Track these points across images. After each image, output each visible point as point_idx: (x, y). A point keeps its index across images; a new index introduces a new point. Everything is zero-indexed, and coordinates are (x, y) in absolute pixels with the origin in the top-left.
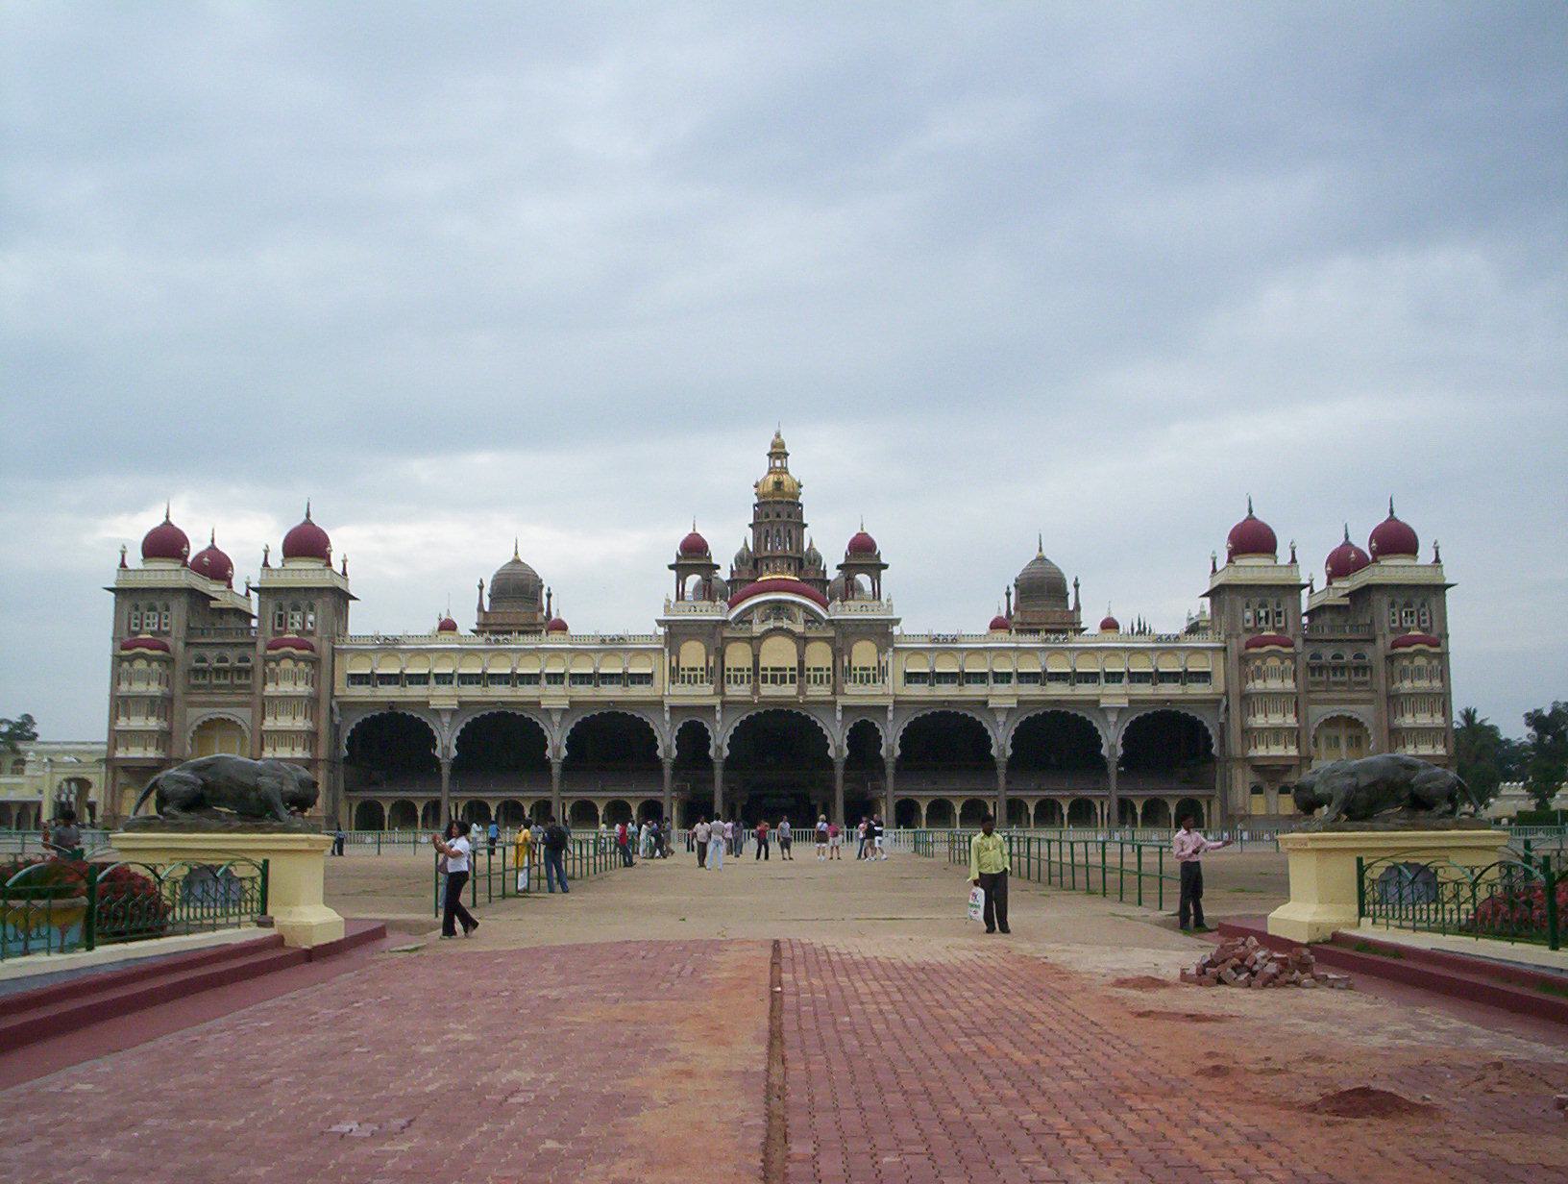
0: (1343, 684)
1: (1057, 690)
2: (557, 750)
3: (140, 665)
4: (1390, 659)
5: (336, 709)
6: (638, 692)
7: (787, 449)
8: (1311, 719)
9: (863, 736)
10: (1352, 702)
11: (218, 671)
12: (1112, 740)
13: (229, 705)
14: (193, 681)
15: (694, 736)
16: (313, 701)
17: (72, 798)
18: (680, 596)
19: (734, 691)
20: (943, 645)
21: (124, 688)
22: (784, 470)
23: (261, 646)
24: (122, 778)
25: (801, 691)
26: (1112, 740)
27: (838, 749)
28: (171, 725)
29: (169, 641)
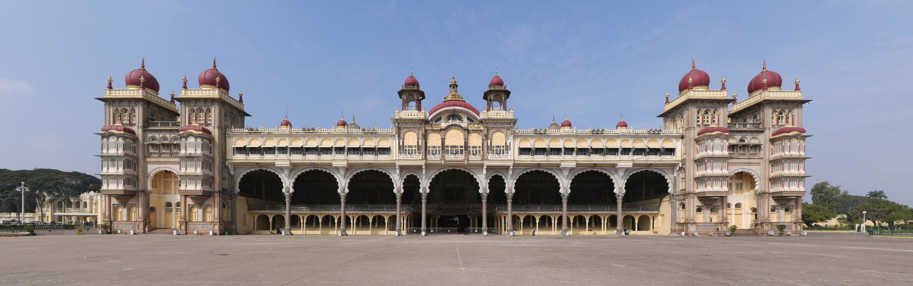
1: (596, 158)
5: (230, 167)
6: (382, 158)
9: (497, 183)
10: (750, 164)
13: (169, 163)
15: (411, 183)
19: (431, 157)
27: (484, 189)
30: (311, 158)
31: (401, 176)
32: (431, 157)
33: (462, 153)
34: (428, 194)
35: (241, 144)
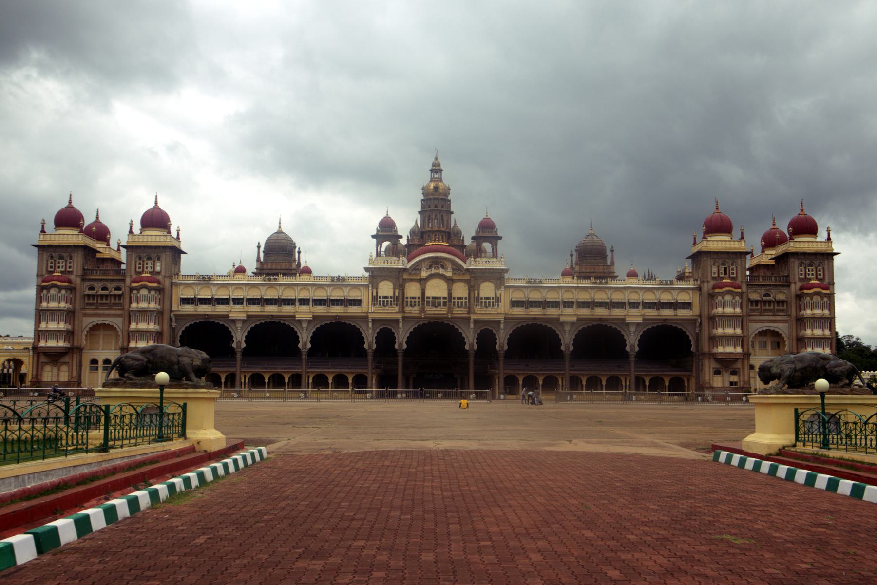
0: (770, 311)
1: (601, 312)
2: (305, 344)
3: (53, 291)
4: (799, 297)
5: (173, 319)
6: (353, 310)
7: (442, 167)
8: (751, 331)
9: (486, 337)
11: (102, 296)
12: (632, 342)
14: (86, 301)
15: (386, 336)
16: (160, 313)
17: (11, 371)
18: (378, 254)
20: (534, 284)
21: (44, 305)
22: (440, 180)
23: (128, 280)
24: (43, 359)
25: (450, 311)
26: (632, 341)
27: (471, 345)
28: (73, 328)
29: (72, 277)
30: (271, 309)
31: (374, 329)
32: (408, 309)
33: (445, 304)
34: (406, 351)
35: (189, 294)
